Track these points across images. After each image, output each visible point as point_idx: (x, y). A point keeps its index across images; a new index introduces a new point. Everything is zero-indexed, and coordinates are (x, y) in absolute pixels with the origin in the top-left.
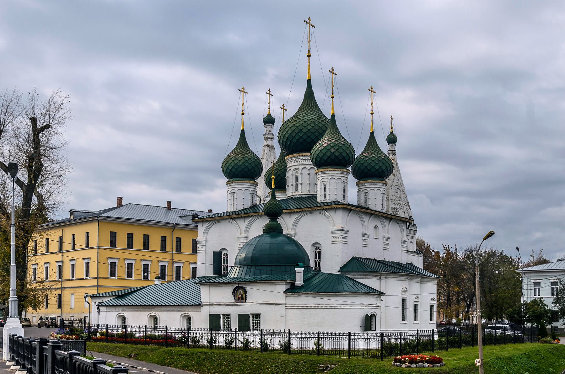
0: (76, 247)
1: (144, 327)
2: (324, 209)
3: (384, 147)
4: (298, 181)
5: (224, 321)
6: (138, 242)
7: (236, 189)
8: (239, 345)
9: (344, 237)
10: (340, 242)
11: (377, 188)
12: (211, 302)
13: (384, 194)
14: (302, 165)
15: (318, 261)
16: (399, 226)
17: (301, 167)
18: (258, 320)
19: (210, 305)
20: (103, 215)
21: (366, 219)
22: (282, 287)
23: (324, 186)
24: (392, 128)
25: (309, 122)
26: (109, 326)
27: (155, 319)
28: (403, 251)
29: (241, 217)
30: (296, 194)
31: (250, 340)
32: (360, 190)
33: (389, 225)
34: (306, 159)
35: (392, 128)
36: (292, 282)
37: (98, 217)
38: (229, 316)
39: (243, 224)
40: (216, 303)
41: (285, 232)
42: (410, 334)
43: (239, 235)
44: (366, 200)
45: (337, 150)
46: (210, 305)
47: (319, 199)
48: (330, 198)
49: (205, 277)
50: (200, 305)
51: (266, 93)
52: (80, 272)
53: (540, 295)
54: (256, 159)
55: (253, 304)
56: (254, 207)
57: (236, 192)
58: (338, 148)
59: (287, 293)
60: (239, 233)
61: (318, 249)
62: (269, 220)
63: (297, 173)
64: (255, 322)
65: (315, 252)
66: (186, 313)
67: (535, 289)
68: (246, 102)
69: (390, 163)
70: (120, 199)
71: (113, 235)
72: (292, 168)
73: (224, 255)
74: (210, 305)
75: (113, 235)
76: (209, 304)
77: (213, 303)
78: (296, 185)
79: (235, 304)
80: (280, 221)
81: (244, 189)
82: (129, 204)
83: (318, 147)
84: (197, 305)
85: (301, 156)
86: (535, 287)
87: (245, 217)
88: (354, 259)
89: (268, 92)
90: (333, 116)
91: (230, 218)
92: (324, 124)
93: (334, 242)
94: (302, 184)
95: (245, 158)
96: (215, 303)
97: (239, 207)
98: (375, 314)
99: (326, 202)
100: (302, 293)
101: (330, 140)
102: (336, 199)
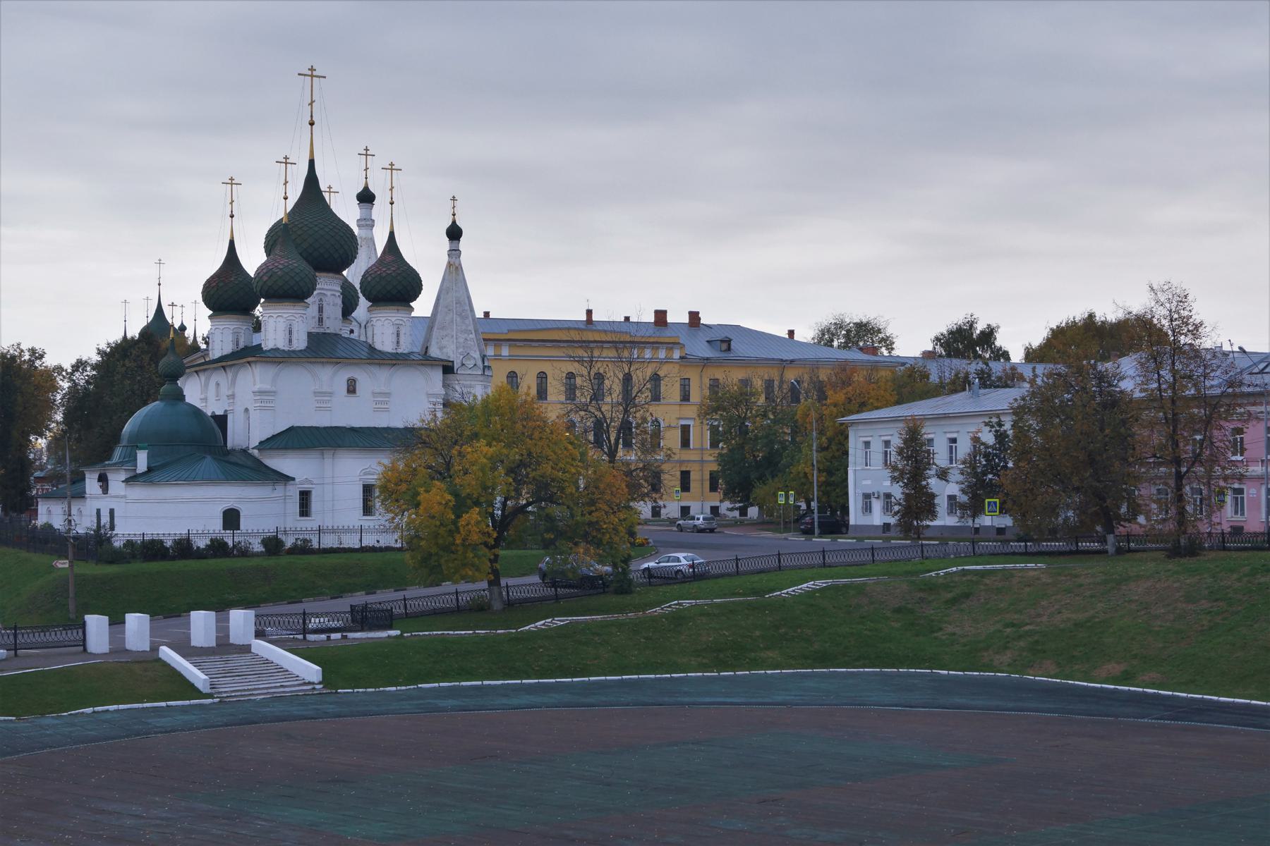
11: (385, 318)
24: (454, 215)
41: (188, 400)
81: (221, 327)
88: (291, 429)
102: (275, 345)
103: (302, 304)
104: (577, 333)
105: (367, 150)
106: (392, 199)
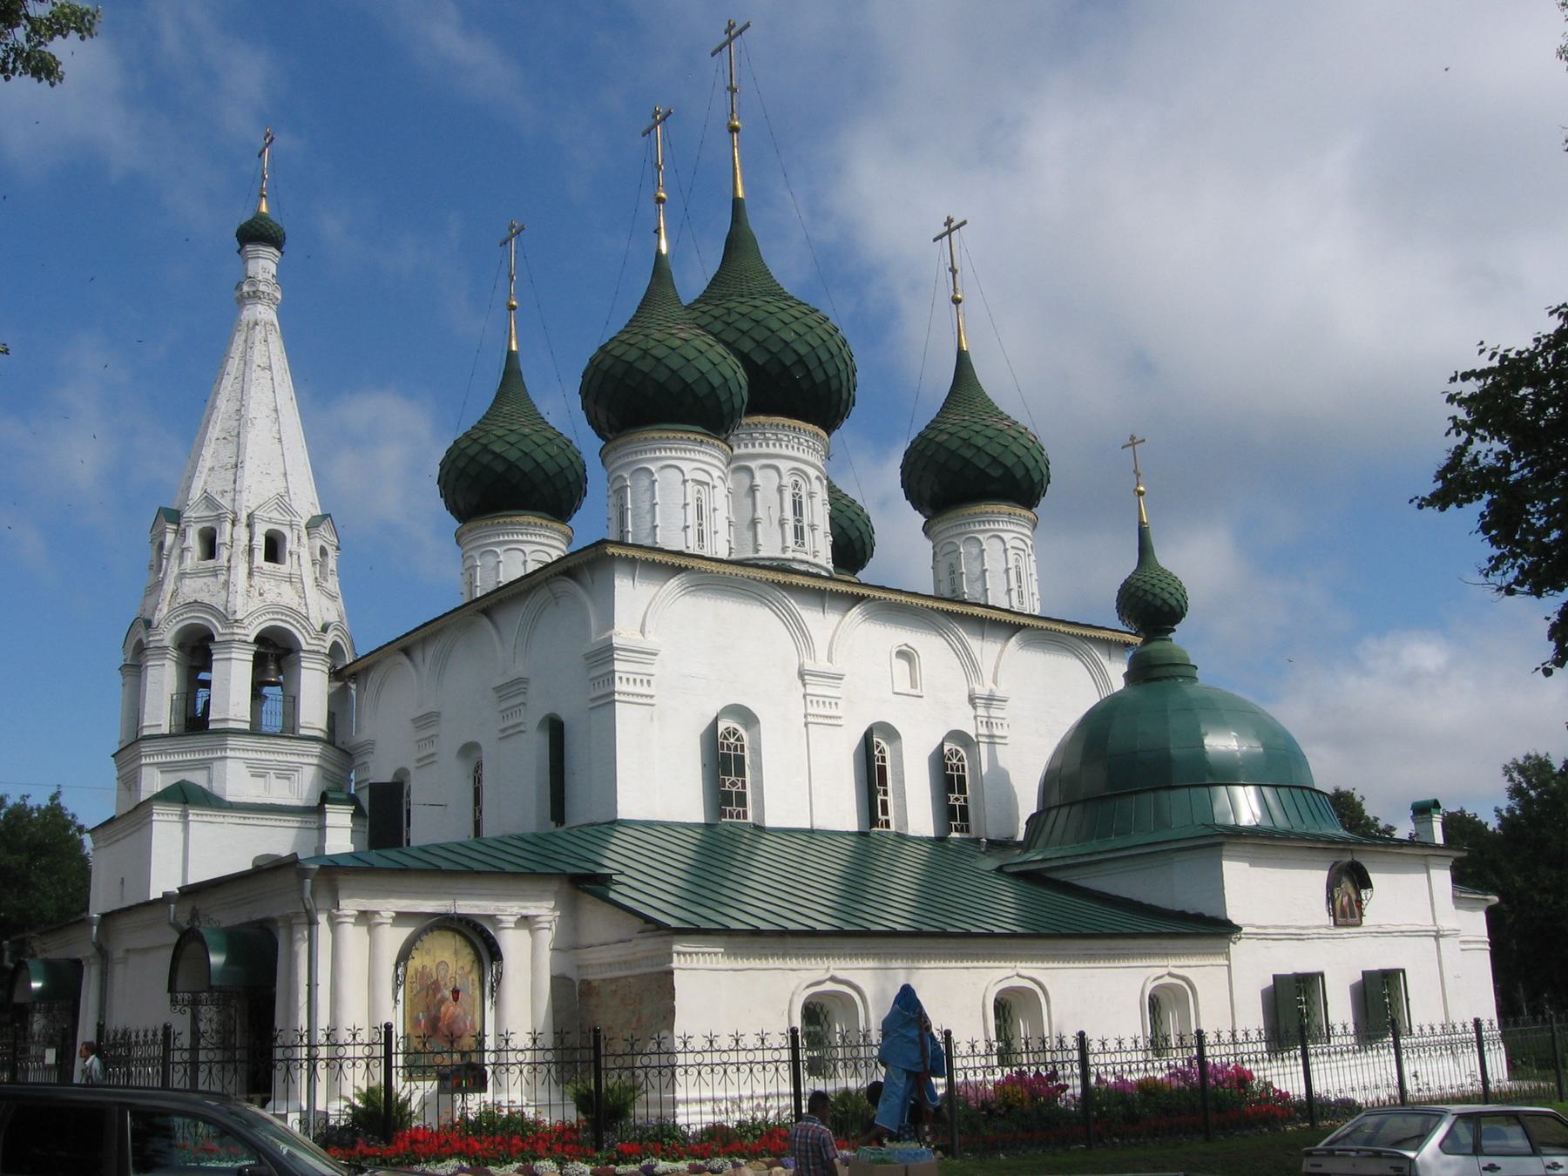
4: (801, 515)
26: (1095, 1046)
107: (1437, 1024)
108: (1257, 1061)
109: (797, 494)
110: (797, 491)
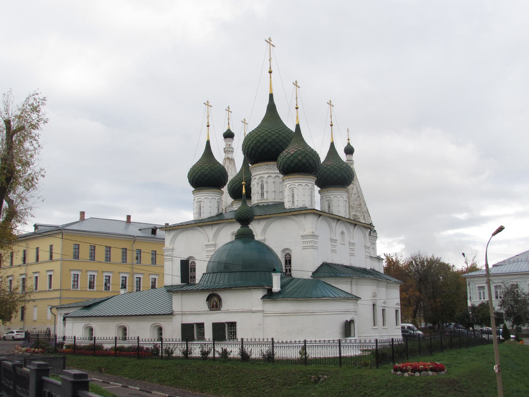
0: (40, 260)
1: (114, 338)
2: (293, 215)
3: (343, 157)
4: (263, 189)
5: (197, 330)
6: (100, 254)
7: (203, 198)
8: (217, 355)
9: (315, 242)
10: (311, 247)
11: (340, 196)
12: (183, 311)
13: (347, 201)
14: (267, 173)
15: (288, 267)
16: (362, 232)
17: (266, 176)
18: (233, 329)
19: (183, 314)
20: (67, 228)
21: (334, 224)
22: (259, 294)
23: (292, 193)
24: (349, 140)
25: (273, 133)
26: (77, 338)
27: (125, 329)
28: (367, 257)
29: (209, 225)
30: (261, 201)
31: (229, 350)
32: (323, 197)
33: (353, 231)
34: (271, 168)
35: (349, 140)
36: (269, 288)
37: (62, 230)
38: (202, 325)
39: (210, 232)
40: (189, 312)
41: (256, 238)
42: (383, 341)
43: (207, 243)
44: (329, 207)
45: (304, 157)
46: (182, 314)
47: (287, 205)
48: (298, 204)
49: (172, 286)
50: (171, 314)
51: (226, 110)
52: (43, 284)
53: (485, 299)
54: (222, 168)
55: (228, 312)
56: (220, 215)
57: (203, 201)
58: (305, 156)
59: (265, 300)
60: (207, 240)
61: (287, 255)
62: (240, 226)
63: (262, 181)
64: (230, 330)
65: (285, 258)
66: (156, 323)
67: (480, 293)
68: (210, 114)
69: (351, 172)
70: (82, 214)
71: (77, 248)
72: (257, 177)
73: (191, 264)
74: (183, 314)
75: (77, 248)
76: (181, 313)
77: (186, 312)
78: (261, 193)
79: (209, 312)
80: (251, 226)
81: (210, 198)
82: (91, 218)
83: (285, 154)
84: (168, 314)
85: (266, 165)
86: (480, 291)
87: (212, 225)
88: (325, 265)
89: (228, 109)
90: (298, 127)
91: (198, 226)
92: (288, 134)
93: (305, 248)
94: (267, 192)
95: (211, 167)
96: (187, 312)
97: (205, 215)
98: (354, 319)
99: (294, 208)
100: (281, 299)
101: (297, 148)
102: (304, 205)
103: (219, 191)
104: (360, 221)
105: (229, 108)
106: (331, 122)
107: (253, 339)
108: (121, 343)
109: (262, 184)
110: (262, 183)
